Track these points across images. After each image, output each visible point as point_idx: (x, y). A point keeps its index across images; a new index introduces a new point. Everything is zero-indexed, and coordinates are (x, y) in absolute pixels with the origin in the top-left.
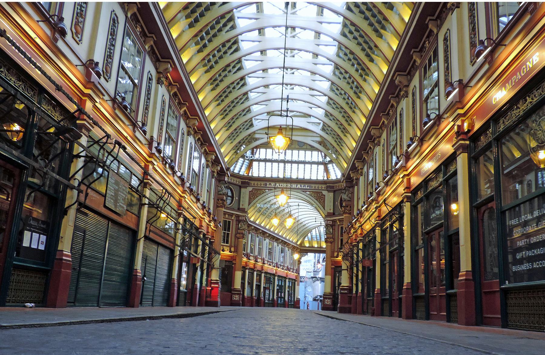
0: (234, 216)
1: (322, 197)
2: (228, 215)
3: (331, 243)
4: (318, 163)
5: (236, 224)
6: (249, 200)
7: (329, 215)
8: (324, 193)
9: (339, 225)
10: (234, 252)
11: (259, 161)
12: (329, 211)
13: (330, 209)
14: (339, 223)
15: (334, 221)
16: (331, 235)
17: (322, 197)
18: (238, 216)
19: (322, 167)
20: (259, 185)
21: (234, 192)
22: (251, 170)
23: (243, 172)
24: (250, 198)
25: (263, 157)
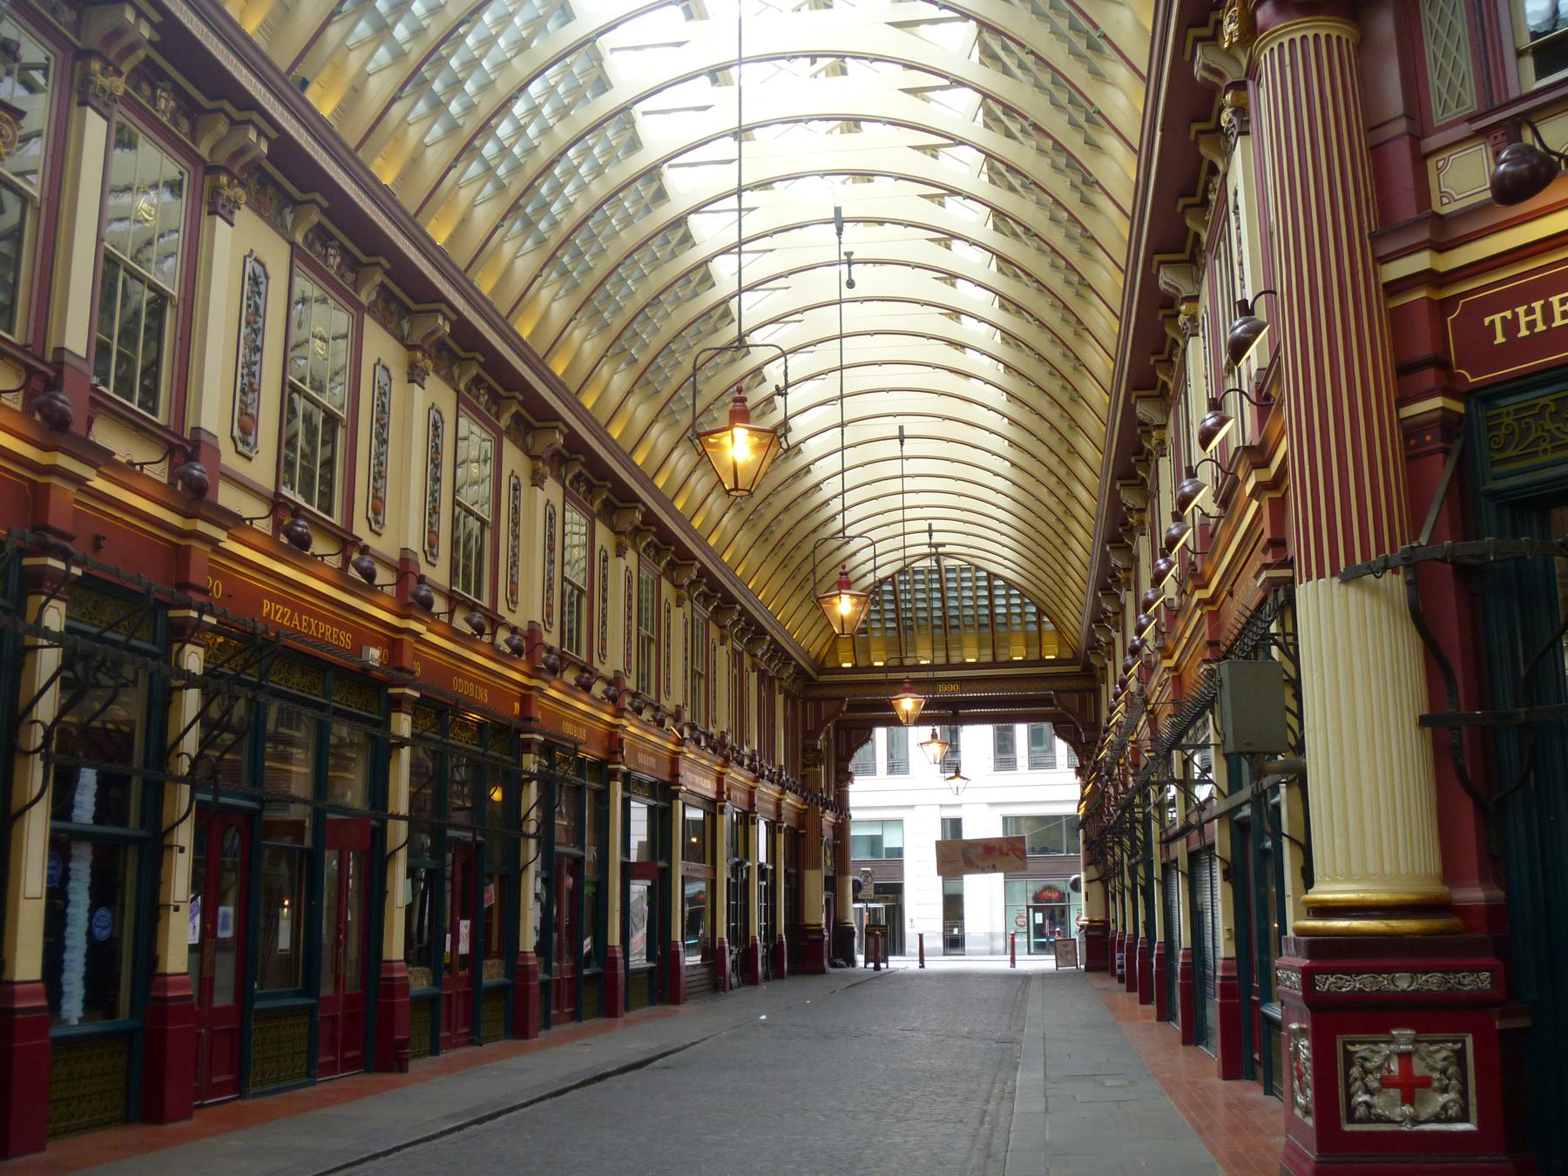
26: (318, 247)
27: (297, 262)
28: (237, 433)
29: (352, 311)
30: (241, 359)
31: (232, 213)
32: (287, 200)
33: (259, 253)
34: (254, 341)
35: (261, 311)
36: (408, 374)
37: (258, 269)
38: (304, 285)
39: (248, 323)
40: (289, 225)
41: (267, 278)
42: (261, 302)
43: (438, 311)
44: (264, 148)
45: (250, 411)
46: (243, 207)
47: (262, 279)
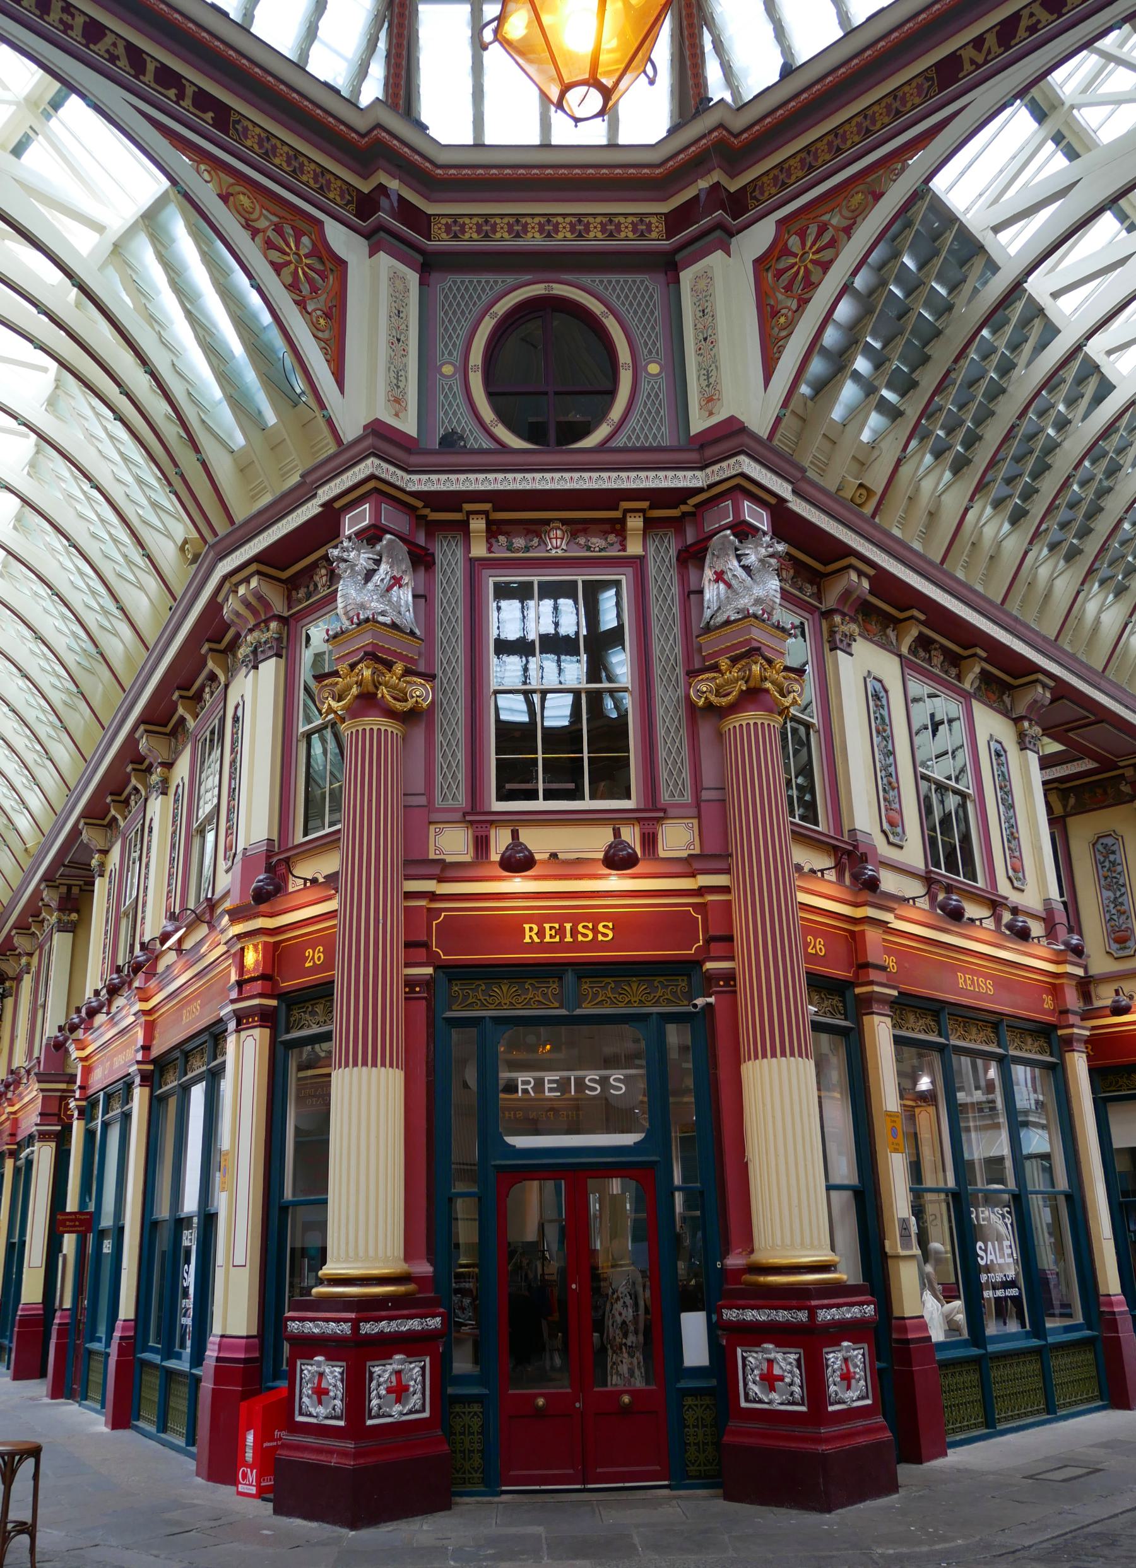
0: (635, 523)
10: (689, 866)
26: (922, 654)
27: (907, 671)
28: (886, 826)
29: (962, 700)
30: (878, 765)
31: (849, 645)
32: (889, 621)
33: (876, 672)
34: (886, 746)
35: (887, 721)
36: (1019, 743)
37: (878, 686)
38: (917, 688)
39: (878, 732)
40: (894, 642)
41: (886, 691)
42: (885, 713)
43: (1037, 681)
44: (866, 584)
45: (894, 806)
46: (858, 638)
47: (883, 694)
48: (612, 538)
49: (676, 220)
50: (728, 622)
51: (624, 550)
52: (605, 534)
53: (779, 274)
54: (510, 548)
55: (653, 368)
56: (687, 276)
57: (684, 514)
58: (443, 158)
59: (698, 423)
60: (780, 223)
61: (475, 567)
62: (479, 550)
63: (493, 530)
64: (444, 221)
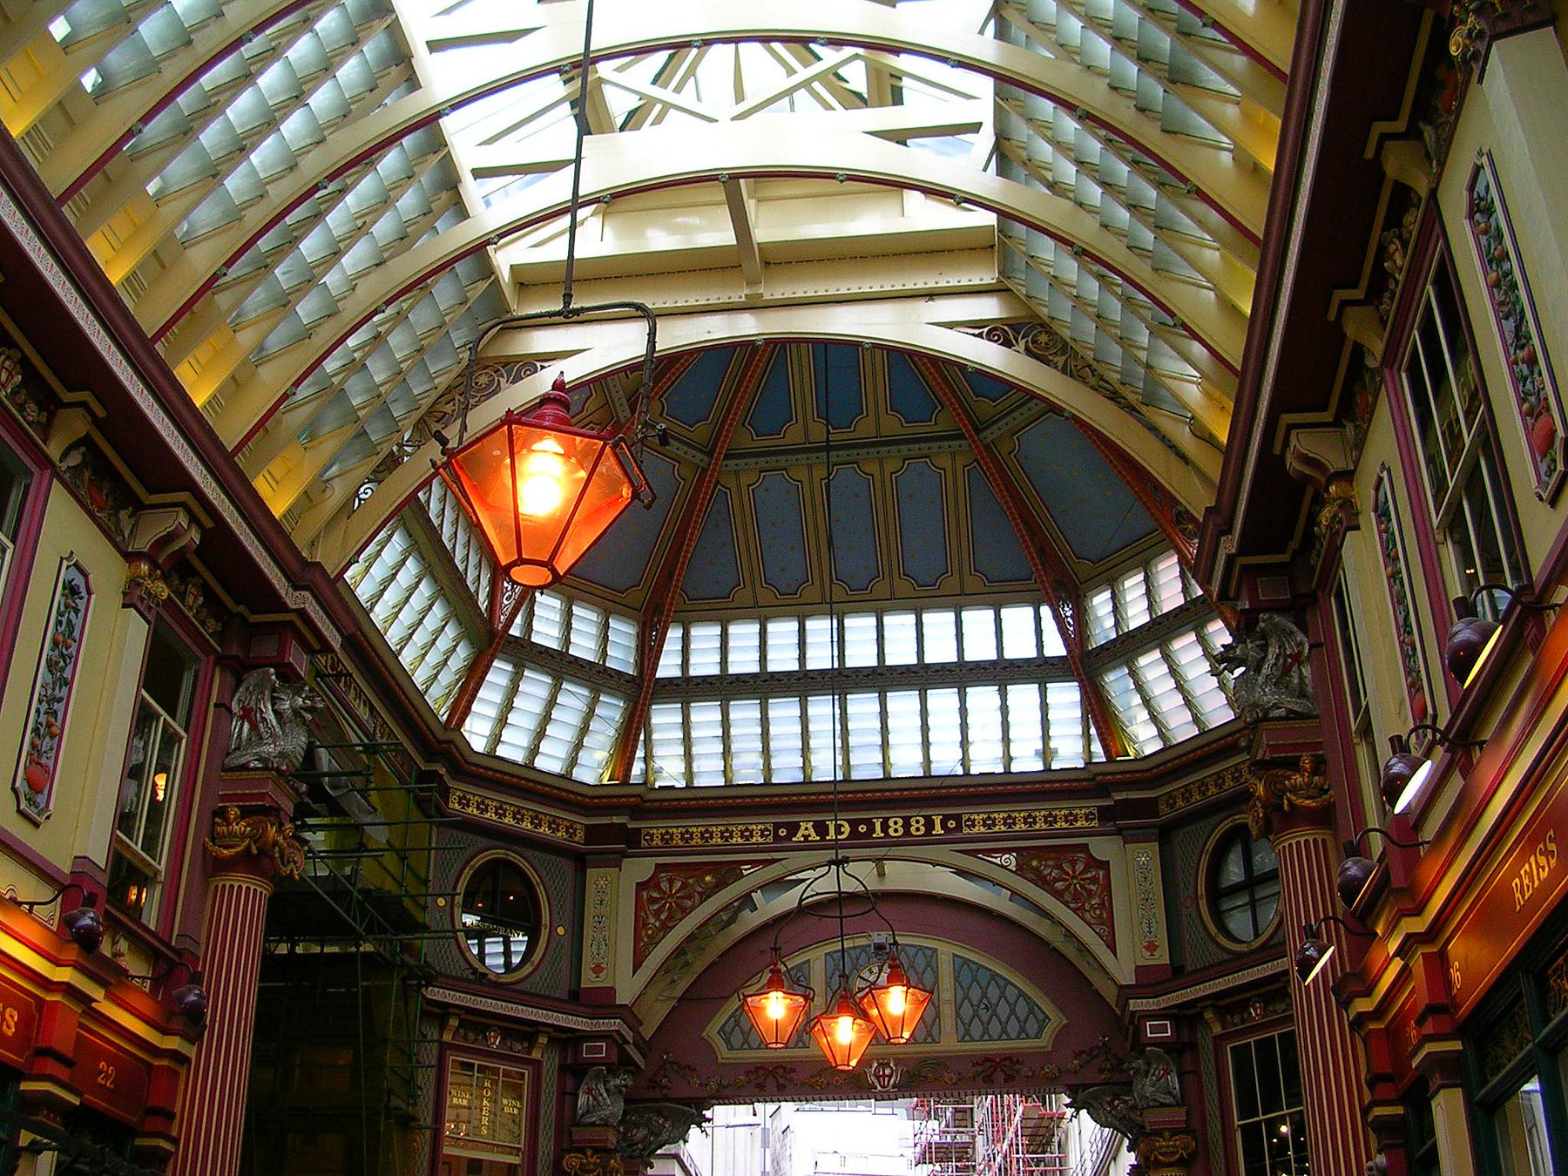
0: (543, 1040)
1: (1094, 880)
2: (507, 1034)
3: (1182, 1163)
4: (1039, 671)
5: (562, 1094)
6: (637, 939)
7: (1149, 983)
8: (1103, 848)
9: (1219, 1040)
11: (688, 690)
12: (1146, 959)
13: (1151, 947)
14: (1217, 1029)
15: (1185, 1016)
16: (1179, 1115)
17: (1094, 880)
18: (567, 1040)
19: (1066, 697)
20: (697, 841)
21: (540, 890)
22: (640, 753)
23: (593, 769)
24: (640, 924)
25: (705, 664)
48: (526, 1045)
49: (592, 833)
50: (593, 1124)
51: (529, 1053)
52: (521, 1041)
53: (652, 900)
54: (465, 1038)
55: (561, 931)
56: (592, 873)
57: (569, 1038)
58: (473, 759)
59: (588, 980)
60: (657, 865)
61: (444, 1047)
62: (447, 1037)
63: (462, 1024)
64: (458, 793)
